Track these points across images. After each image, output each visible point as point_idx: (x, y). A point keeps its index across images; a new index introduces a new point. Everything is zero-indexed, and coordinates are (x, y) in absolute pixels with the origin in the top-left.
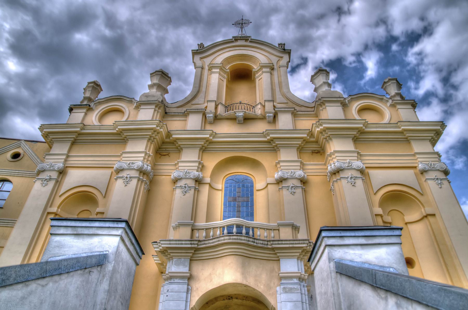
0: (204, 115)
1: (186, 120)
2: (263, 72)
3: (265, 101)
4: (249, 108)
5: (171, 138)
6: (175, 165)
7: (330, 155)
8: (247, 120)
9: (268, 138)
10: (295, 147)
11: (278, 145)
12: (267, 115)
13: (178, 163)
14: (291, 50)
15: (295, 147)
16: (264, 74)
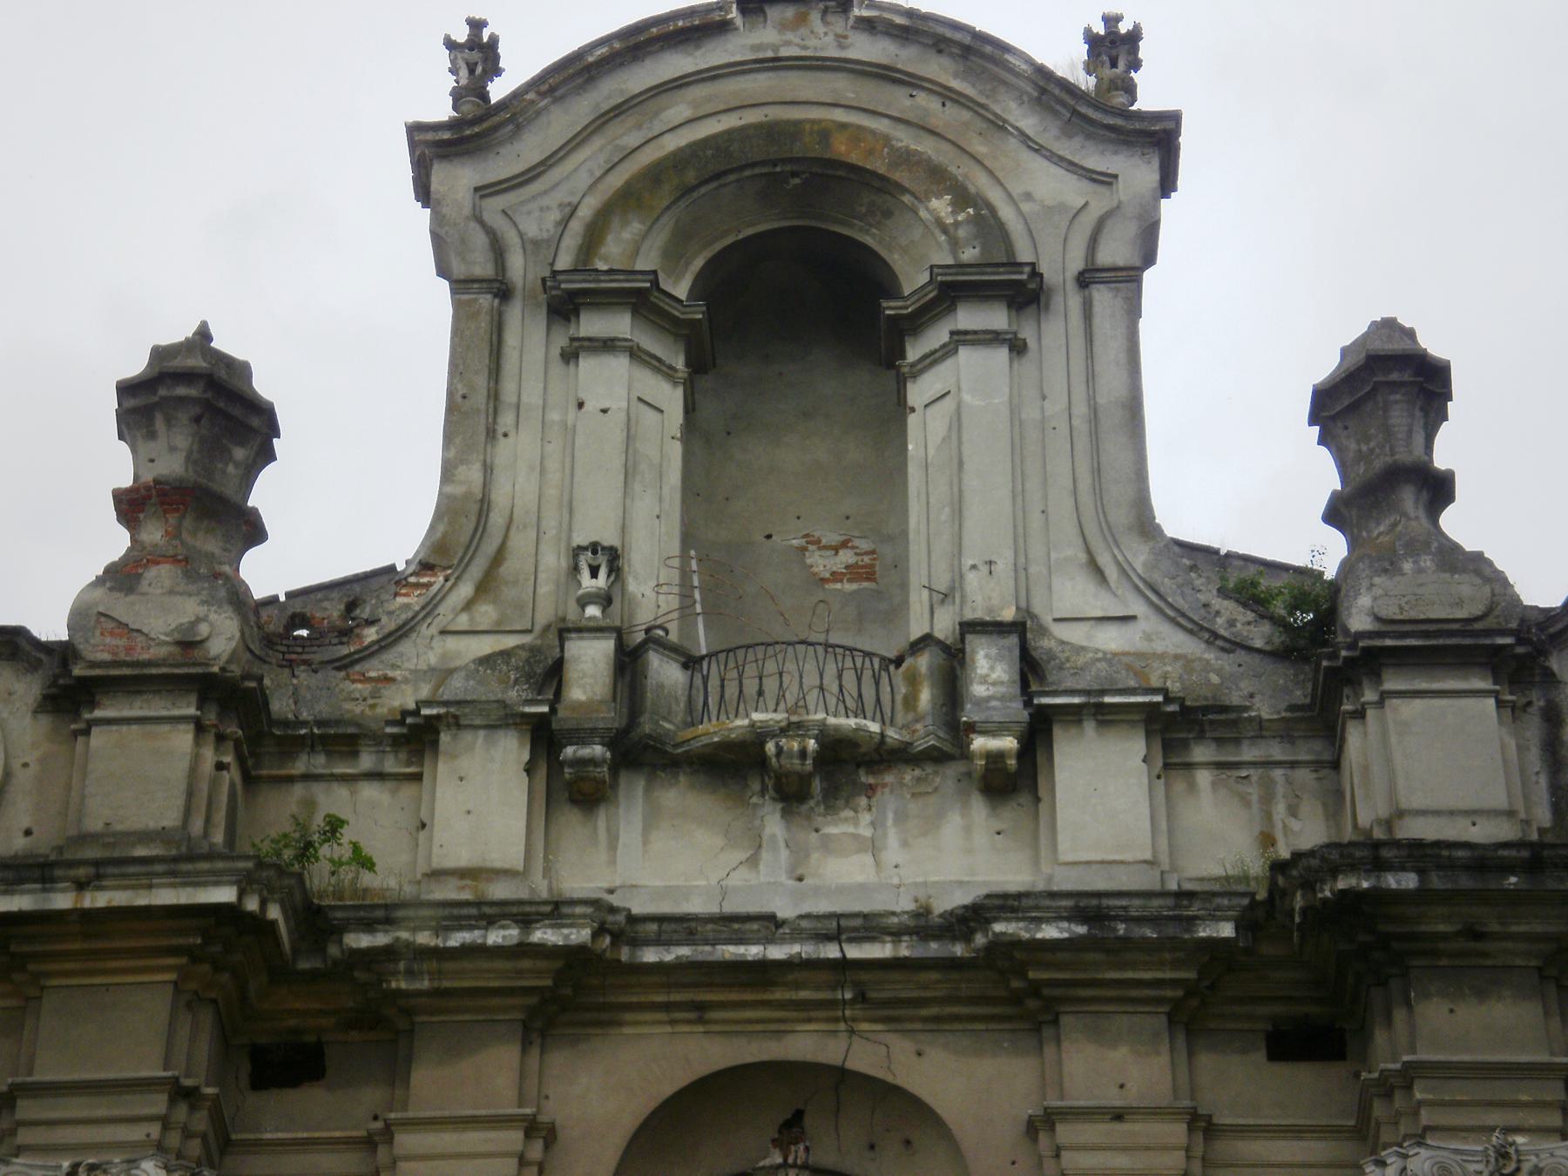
0: (545, 738)
1: (417, 777)
2: (961, 338)
3: (970, 627)
4: (849, 679)
5: (333, 950)
6: (369, 1143)
7: (1387, 1087)
8: (844, 769)
9: (980, 940)
10: (1159, 1001)
11: (1046, 992)
12: (979, 743)
13: (388, 1133)
14: (1175, 118)
15: (1159, 1001)
16: (964, 353)
